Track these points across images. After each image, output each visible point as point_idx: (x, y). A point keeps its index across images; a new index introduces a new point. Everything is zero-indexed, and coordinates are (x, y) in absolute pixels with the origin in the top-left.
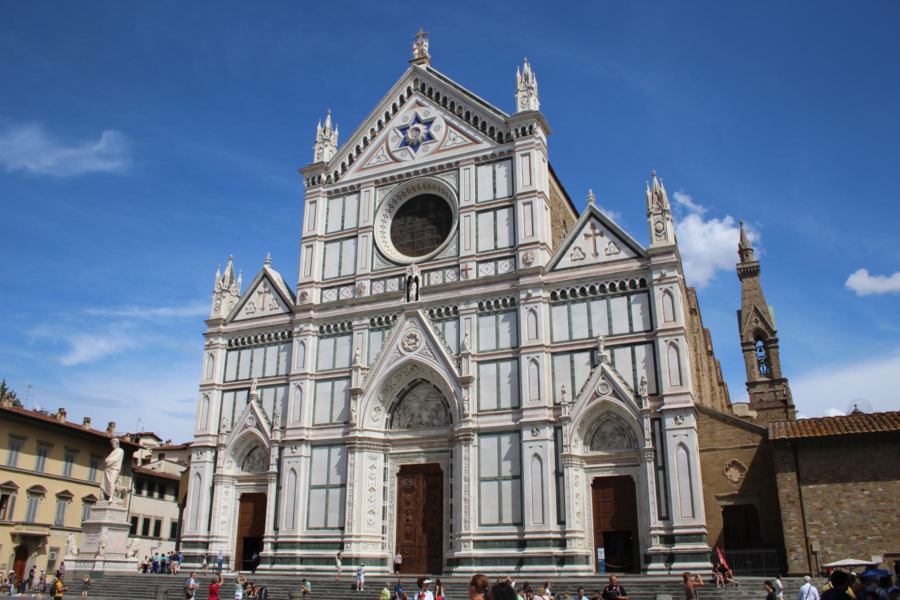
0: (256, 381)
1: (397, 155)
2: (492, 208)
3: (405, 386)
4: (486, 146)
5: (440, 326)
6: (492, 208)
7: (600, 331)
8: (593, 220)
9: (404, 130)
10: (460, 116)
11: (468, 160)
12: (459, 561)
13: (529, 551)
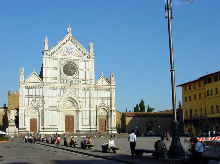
0: (34, 96)
1: (66, 54)
2: (85, 70)
3: (67, 101)
4: (84, 58)
5: (75, 91)
6: (85, 70)
7: (102, 96)
8: (102, 77)
9: (67, 49)
10: (79, 50)
11: (81, 60)
12: (80, 131)
13: (91, 130)
